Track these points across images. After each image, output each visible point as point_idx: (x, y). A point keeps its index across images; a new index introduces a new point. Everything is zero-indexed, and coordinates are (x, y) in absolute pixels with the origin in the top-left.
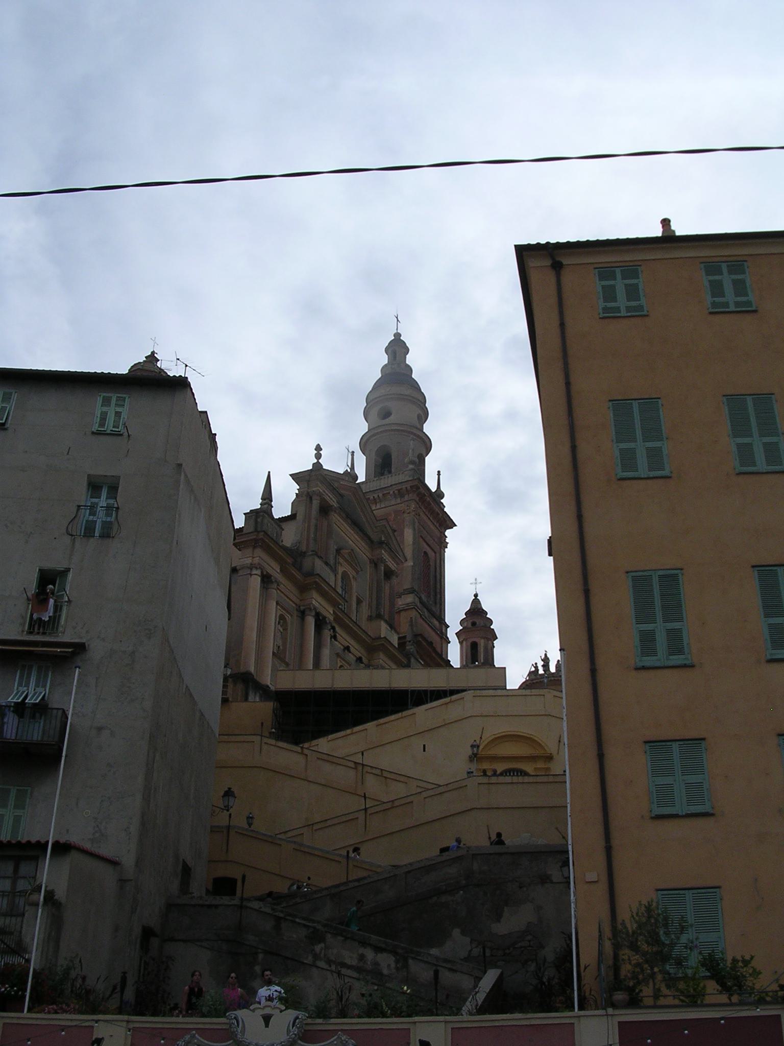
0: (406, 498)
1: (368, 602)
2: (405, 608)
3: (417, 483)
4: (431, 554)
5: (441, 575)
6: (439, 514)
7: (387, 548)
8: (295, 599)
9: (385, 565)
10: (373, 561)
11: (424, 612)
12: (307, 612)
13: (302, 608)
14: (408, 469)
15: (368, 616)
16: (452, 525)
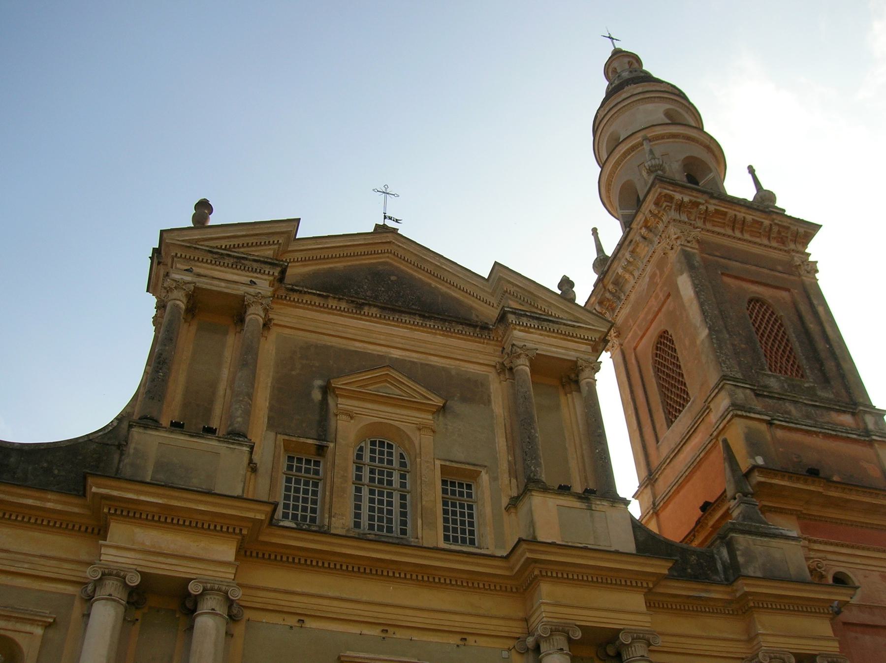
0: (661, 226)
2: (721, 427)
3: (659, 190)
5: (820, 324)
6: (762, 222)
7: (524, 320)
9: (531, 360)
11: (789, 413)
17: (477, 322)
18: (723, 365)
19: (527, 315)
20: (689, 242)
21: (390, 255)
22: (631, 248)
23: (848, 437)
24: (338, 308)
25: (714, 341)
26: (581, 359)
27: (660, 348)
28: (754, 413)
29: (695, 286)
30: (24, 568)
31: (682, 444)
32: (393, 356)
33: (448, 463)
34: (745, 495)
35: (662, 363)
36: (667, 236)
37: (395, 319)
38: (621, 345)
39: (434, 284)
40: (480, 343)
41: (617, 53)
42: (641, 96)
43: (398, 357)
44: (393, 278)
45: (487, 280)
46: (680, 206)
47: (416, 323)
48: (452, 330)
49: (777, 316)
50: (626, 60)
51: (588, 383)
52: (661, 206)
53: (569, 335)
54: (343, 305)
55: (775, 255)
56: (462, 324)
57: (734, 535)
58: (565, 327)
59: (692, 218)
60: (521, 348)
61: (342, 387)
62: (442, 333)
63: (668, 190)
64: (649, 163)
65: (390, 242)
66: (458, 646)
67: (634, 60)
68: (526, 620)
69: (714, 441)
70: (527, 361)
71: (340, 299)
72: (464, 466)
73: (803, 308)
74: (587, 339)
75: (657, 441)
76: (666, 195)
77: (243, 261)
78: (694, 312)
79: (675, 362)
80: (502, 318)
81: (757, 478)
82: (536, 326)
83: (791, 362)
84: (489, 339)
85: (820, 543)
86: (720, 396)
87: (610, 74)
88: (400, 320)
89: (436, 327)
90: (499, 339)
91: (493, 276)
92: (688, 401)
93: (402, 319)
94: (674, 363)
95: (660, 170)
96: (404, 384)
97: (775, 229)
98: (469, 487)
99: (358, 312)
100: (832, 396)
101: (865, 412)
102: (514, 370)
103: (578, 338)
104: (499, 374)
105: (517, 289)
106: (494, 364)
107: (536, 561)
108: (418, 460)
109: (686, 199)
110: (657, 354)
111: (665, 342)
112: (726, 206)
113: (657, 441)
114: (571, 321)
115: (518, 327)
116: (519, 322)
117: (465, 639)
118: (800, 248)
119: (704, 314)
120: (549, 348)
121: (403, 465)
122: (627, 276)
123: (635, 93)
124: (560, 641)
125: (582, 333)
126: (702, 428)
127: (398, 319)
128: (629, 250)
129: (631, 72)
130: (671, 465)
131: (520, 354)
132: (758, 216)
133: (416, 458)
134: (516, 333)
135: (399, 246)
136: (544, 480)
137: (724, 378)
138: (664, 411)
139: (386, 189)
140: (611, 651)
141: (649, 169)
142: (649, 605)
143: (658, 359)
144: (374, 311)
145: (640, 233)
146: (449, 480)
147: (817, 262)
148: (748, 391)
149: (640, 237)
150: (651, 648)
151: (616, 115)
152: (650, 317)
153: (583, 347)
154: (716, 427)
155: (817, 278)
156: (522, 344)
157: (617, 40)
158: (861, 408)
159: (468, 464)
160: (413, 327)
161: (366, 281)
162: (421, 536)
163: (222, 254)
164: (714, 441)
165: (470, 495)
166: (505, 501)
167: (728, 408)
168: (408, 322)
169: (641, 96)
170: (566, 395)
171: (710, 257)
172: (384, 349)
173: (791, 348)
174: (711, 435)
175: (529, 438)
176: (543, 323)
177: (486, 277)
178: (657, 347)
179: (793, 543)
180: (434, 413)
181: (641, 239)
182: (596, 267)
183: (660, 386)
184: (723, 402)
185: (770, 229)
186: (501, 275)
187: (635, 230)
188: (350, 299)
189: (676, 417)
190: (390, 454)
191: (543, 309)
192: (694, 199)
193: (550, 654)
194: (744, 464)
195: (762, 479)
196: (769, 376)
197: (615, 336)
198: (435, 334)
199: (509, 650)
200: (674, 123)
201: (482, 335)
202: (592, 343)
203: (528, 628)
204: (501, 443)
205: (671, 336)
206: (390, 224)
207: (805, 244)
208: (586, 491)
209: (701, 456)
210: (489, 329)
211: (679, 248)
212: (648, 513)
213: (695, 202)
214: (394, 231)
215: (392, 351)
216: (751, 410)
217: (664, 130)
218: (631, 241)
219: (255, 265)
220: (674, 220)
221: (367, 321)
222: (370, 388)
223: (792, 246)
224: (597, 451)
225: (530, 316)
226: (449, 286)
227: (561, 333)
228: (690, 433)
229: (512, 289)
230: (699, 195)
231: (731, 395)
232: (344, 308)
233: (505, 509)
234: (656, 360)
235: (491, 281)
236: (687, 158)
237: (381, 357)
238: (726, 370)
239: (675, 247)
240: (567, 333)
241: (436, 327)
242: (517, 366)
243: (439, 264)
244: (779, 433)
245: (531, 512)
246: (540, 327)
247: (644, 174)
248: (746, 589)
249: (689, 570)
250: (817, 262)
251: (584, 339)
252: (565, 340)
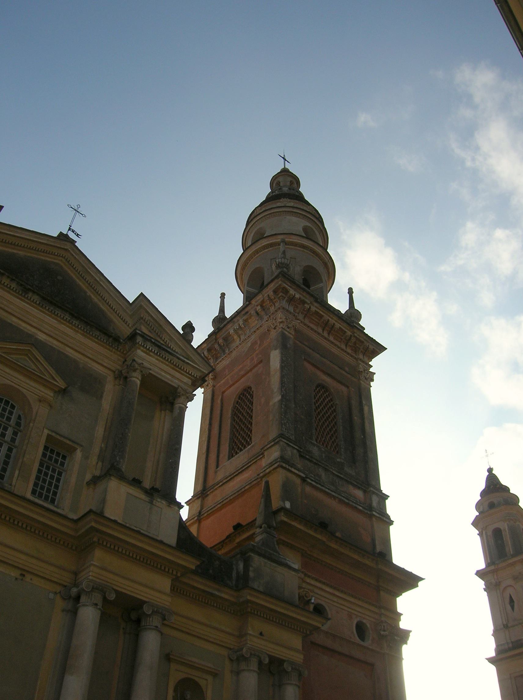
0: (272, 309)
2: (267, 471)
3: (280, 283)
6: (346, 332)
7: (149, 345)
9: (143, 376)
16: (378, 348)
17: (112, 333)
18: (283, 426)
19: (152, 342)
20: (288, 328)
21: (63, 259)
22: (245, 317)
23: (356, 507)
24: (8, 286)
25: (283, 406)
26: (181, 388)
27: (242, 398)
28: (295, 469)
29: (282, 361)
31: (234, 475)
32: (38, 337)
33: (54, 434)
34: (270, 527)
35: (239, 410)
36: (274, 318)
37: (50, 310)
38: (214, 386)
39: (89, 293)
40: (109, 350)
41: (285, 172)
42: (291, 210)
43: (42, 339)
44: (60, 278)
46: (291, 300)
47: (65, 318)
48: (91, 333)
49: (333, 403)
50: (289, 179)
51: (180, 407)
52: (278, 295)
53: (178, 367)
54: (14, 285)
55: (347, 358)
56: (100, 331)
57: (252, 555)
58: (177, 360)
59: (297, 311)
60: (140, 364)
62: (82, 332)
63: (287, 285)
64: (280, 260)
65: (66, 250)
66: (16, 579)
67: (295, 181)
68: (76, 574)
69: (259, 480)
70: (140, 375)
71: (12, 280)
72: (65, 440)
73: (354, 403)
74: (191, 375)
75: (217, 467)
76: (284, 288)
78: (275, 380)
79: (250, 412)
80: (132, 337)
81: (283, 517)
82: (156, 352)
83: (333, 440)
84: (117, 350)
85: (313, 578)
86: (274, 448)
87: (274, 185)
88: (53, 312)
89: (80, 326)
90: (125, 352)
91: (137, 302)
92: (249, 444)
93: (55, 312)
94: (248, 413)
95: (286, 268)
96: (39, 361)
97: (353, 340)
98: (64, 457)
99: (23, 294)
100: (354, 474)
101: (374, 493)
102: (128, 380)
103: (184, 371)
104: (116, 378)
106: (113, 369)
107: (98, 531)
108: (31, 424)
109: (297, 296)
110: (238, 402)
111: (247, 395)
112: (324, 311)
113: (217, 467)
114: (183, 356)
115: (142, 348)
116: (144, 345)
117: (24, 575)
118: (366, 359)
119: (282, 384)
120: (159, 371)
121: (18, 424)
122: (235, 337)
123: (287, 205)
124: (97, 598)
126: (253, 467)
127: (52, 310)
128: (243, 318)
129: (290, 189)
130: (222, 488)
131: (137, 369)
132: (344, 326)
133: (30, 423)
134: (140, 352)
135: (73, 255)
136: (123, 470)
137: (281, 436)
138: (229, 445)
139: (78, 208)
140: (134, 616)
142: (174, 589)
143: (237, 406)
144: (36, 298)
145: (256, 309)
146: (50, 448)
147: (375, 374)
148: (295, 451)
149: (254, 312)
150: (165, 622)
152: (242, 373)
153: (186, 380)
154: (263, 470)
155: (371, 385)
156: (140, 361)
157: (288, 162)
158: (372, 489)
159: (70, 440)
160: (62, 321)
161: (38, 273)
162: (14, 484)
164: (259, 480)
165: (62, 464)
166: (88, 477)
167: (277, 459)
168: (59, 315)
169: (291, 210)
170: (161, 411)
171: (300, 344)
172: (34, 330)
173: (336, 430)
174: (258, 475)
175: (122, 434)
177: (131, 302)
178: (240, 396)
179: (293, 573)
180: (55, 392)
181: (256, 314)
182: (215, 323)
183: (233, 427)
184: (275, 453)
186: (143, 304)
187: (253, 306)
188: (21, 282)
189: (237, 453)
190: (11, 413)
191: (165, 341)
192: (302, 298)
193: (87, 605)
194: (276, 504)
195: (285, 519)
196: (314, 445)
197: (211, 379)
198: (77, 332)
199: (56, 593)
200: (307, 238)
201: (112, 345)
202: (193, 378)
203: (75, 581)
204: (100, 431)
205: (253, 392)
206: (72, 235)
207: (371, 359)
208: (153, 488)
209: (246, 488)
210: (119, 342)
211: (280, 330)
212: (193, 519)
213: (303, 300)
214: (73, 242)
215: (39, 333)
216: (293, 466)
217: (299, 240)
218: (247, 312)
220: (284, 308)
221: (28, 303)
222: (12, 356)
223: (361, 356)
225: (154, 343)
226: (100, 299)
227: (173, 364)
228: (244, 468)
229: (147, 318)
230: (307, 296)
231: (282, 450)
232: (13, 288)
233: (86, 483)
234: (236, 406)
236: (308, 266)
237: (30, 336)
238: (284, 430)
239: (277, 328)
240: (177, 364)
241: (80, 326)
242: (131, 377)
243: (98, 279)
244: (308, 489)
245: (105, 491)
246: (158, 354)
247: (274, 267)
248: (249, 597)
249: (211, 571)
250: (375, 374)
251: (188, 373)
252: (173, 369)
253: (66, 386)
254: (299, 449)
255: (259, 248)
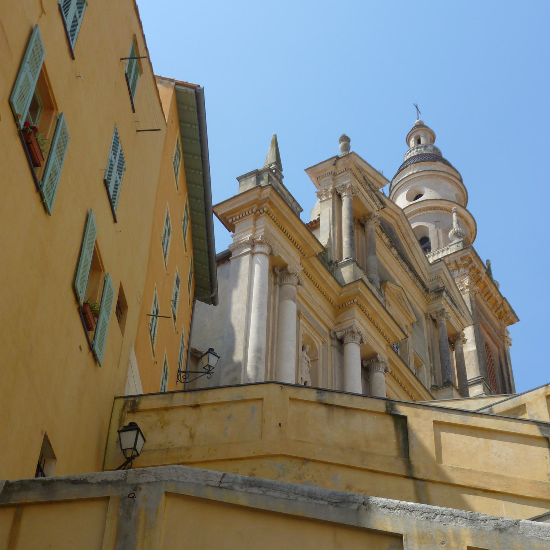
1: (429, 368)
4: (494, 348)
5: (508, 375)
6: (498, 301)
7: (448, 298)
8: (326, 319)
10: (431, 316)
12: (348, 339)
13: (339, 334)
14: (454, 242)
15: (432, 386)
19: (450, 297)
30: (314, 307)
41: (421, 126)
45: (431, 265)
54: (387, 241)
61: (390, 287)
76: (470, 258)
77: (372, 192)
105: (445, 280)
109: (477, 266)
115: (444, 301)
118: (505, 325)
125: (462, 319)
141: (457, 233)
144: (395, 252)
151: (426, 177)
163: (367, 183)
175: (449, 360)
176: (453, 305)
185: (499, 308)
219: (375, 198)
223: (503, 323)
224: (465, 383)
235: (433, 266)
242: (442, 321)
253: (417, 321)
254: (491, 390)
255: (423, 208)
